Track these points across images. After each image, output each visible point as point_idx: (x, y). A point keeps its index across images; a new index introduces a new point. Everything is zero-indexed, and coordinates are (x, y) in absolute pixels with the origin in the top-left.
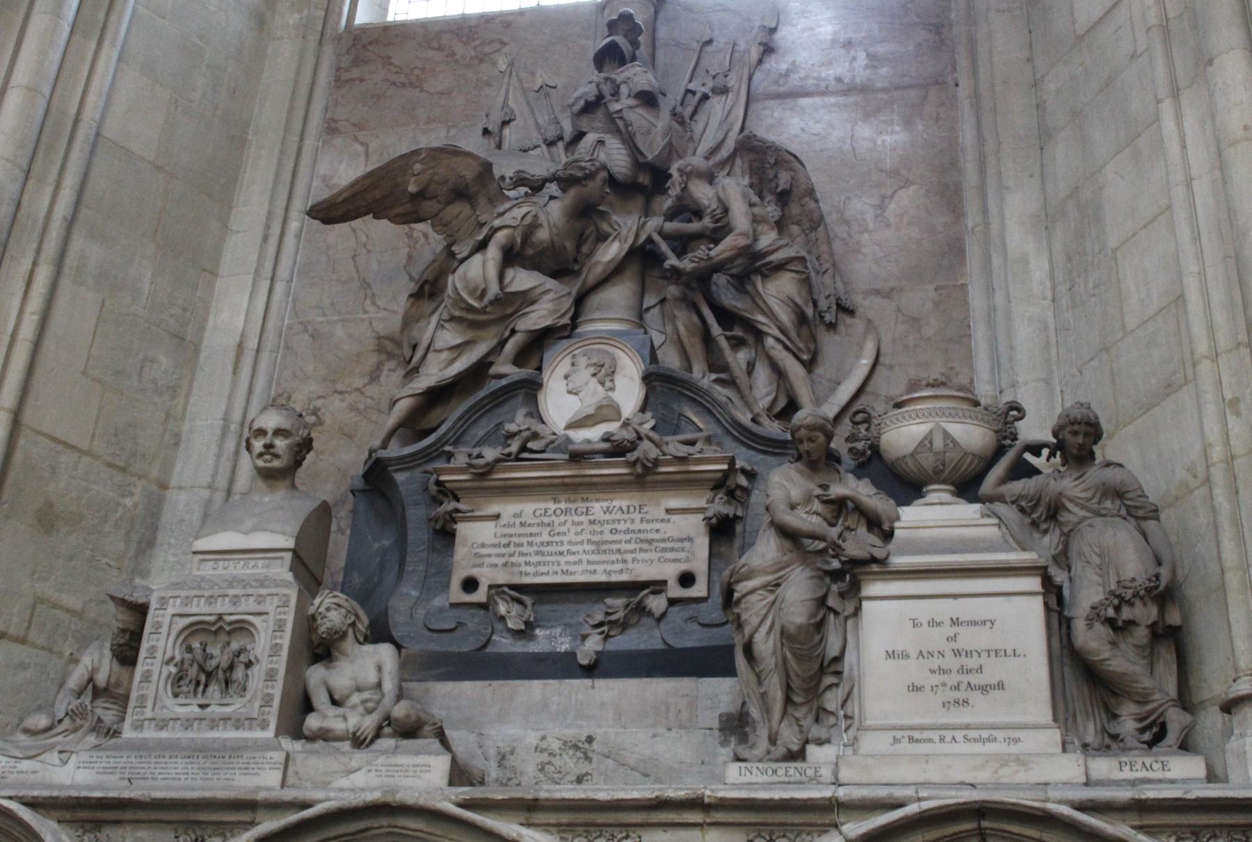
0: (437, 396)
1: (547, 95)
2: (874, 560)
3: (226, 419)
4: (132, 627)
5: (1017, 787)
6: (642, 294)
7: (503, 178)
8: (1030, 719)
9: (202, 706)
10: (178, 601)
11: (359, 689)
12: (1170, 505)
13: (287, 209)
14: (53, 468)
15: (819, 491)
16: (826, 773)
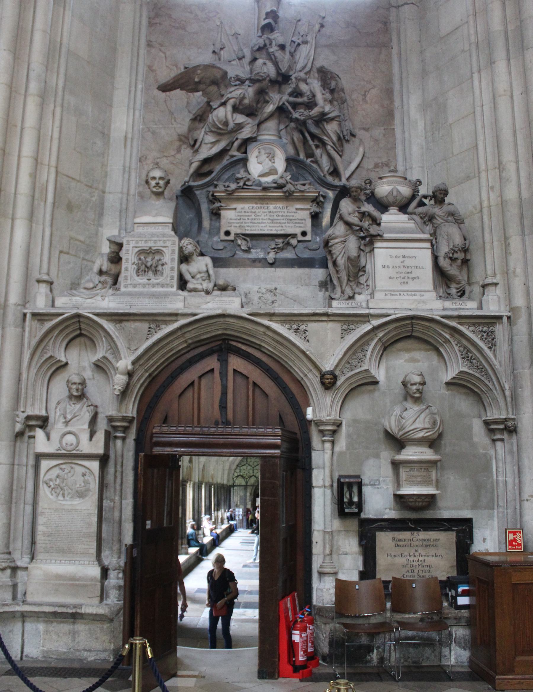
0: (206, 161)
1: (237, 38)
2: (379, 235)
3: (124, 166)
4: (117, 251)
5: (423, 310)
6: (279, 123)
7: (231, 78)
8: (426, 289)
9: (149, 280)
10: (134, 242)
11: (200, 273)
12: (467, 218)
13: (136, 80)
14: (69, 187)
15: (357, 209)
16: (364, 305)
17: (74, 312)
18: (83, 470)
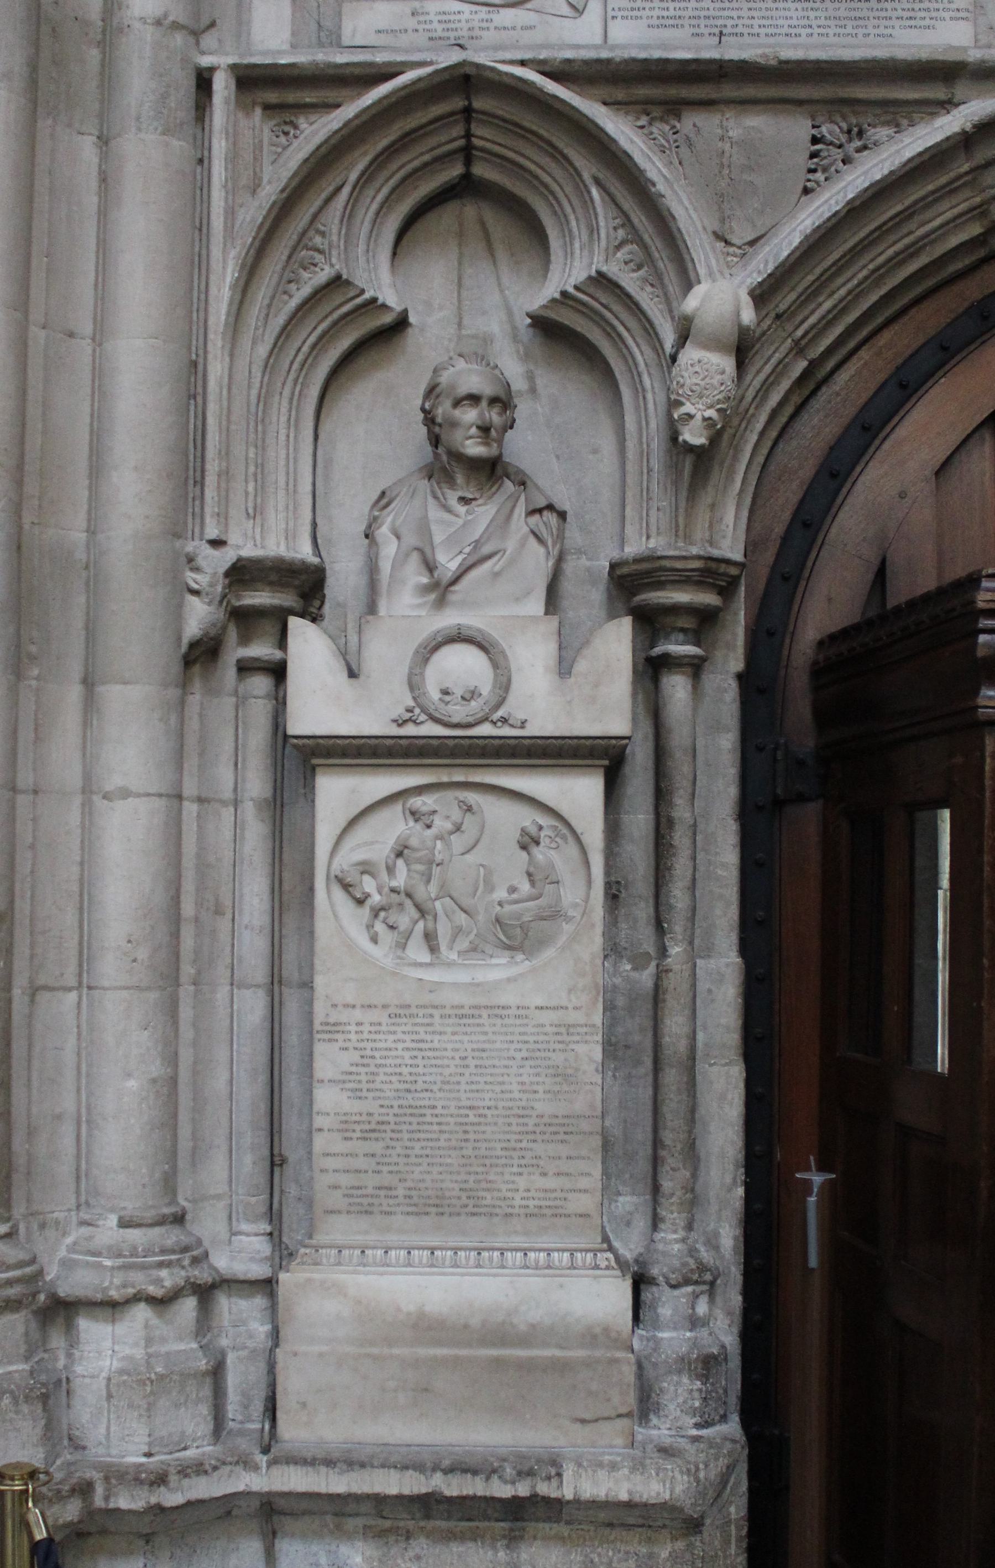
17: (452, 57)
18: (527, 818)
